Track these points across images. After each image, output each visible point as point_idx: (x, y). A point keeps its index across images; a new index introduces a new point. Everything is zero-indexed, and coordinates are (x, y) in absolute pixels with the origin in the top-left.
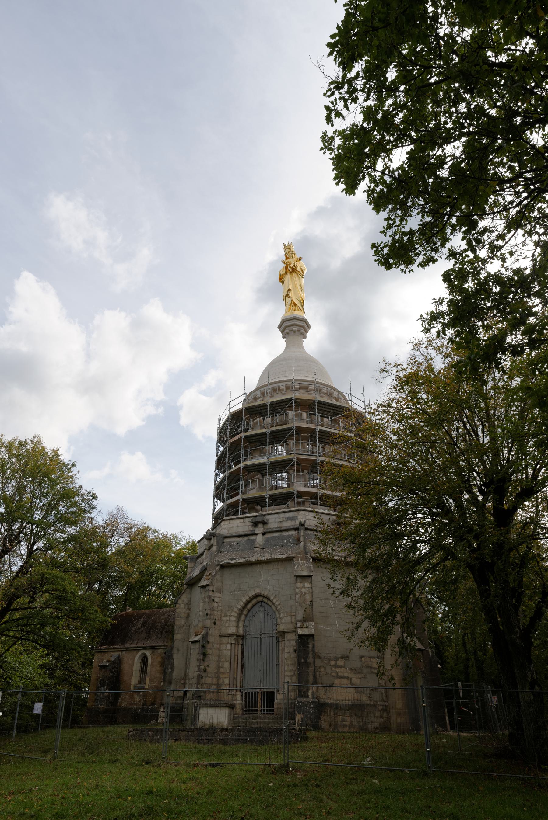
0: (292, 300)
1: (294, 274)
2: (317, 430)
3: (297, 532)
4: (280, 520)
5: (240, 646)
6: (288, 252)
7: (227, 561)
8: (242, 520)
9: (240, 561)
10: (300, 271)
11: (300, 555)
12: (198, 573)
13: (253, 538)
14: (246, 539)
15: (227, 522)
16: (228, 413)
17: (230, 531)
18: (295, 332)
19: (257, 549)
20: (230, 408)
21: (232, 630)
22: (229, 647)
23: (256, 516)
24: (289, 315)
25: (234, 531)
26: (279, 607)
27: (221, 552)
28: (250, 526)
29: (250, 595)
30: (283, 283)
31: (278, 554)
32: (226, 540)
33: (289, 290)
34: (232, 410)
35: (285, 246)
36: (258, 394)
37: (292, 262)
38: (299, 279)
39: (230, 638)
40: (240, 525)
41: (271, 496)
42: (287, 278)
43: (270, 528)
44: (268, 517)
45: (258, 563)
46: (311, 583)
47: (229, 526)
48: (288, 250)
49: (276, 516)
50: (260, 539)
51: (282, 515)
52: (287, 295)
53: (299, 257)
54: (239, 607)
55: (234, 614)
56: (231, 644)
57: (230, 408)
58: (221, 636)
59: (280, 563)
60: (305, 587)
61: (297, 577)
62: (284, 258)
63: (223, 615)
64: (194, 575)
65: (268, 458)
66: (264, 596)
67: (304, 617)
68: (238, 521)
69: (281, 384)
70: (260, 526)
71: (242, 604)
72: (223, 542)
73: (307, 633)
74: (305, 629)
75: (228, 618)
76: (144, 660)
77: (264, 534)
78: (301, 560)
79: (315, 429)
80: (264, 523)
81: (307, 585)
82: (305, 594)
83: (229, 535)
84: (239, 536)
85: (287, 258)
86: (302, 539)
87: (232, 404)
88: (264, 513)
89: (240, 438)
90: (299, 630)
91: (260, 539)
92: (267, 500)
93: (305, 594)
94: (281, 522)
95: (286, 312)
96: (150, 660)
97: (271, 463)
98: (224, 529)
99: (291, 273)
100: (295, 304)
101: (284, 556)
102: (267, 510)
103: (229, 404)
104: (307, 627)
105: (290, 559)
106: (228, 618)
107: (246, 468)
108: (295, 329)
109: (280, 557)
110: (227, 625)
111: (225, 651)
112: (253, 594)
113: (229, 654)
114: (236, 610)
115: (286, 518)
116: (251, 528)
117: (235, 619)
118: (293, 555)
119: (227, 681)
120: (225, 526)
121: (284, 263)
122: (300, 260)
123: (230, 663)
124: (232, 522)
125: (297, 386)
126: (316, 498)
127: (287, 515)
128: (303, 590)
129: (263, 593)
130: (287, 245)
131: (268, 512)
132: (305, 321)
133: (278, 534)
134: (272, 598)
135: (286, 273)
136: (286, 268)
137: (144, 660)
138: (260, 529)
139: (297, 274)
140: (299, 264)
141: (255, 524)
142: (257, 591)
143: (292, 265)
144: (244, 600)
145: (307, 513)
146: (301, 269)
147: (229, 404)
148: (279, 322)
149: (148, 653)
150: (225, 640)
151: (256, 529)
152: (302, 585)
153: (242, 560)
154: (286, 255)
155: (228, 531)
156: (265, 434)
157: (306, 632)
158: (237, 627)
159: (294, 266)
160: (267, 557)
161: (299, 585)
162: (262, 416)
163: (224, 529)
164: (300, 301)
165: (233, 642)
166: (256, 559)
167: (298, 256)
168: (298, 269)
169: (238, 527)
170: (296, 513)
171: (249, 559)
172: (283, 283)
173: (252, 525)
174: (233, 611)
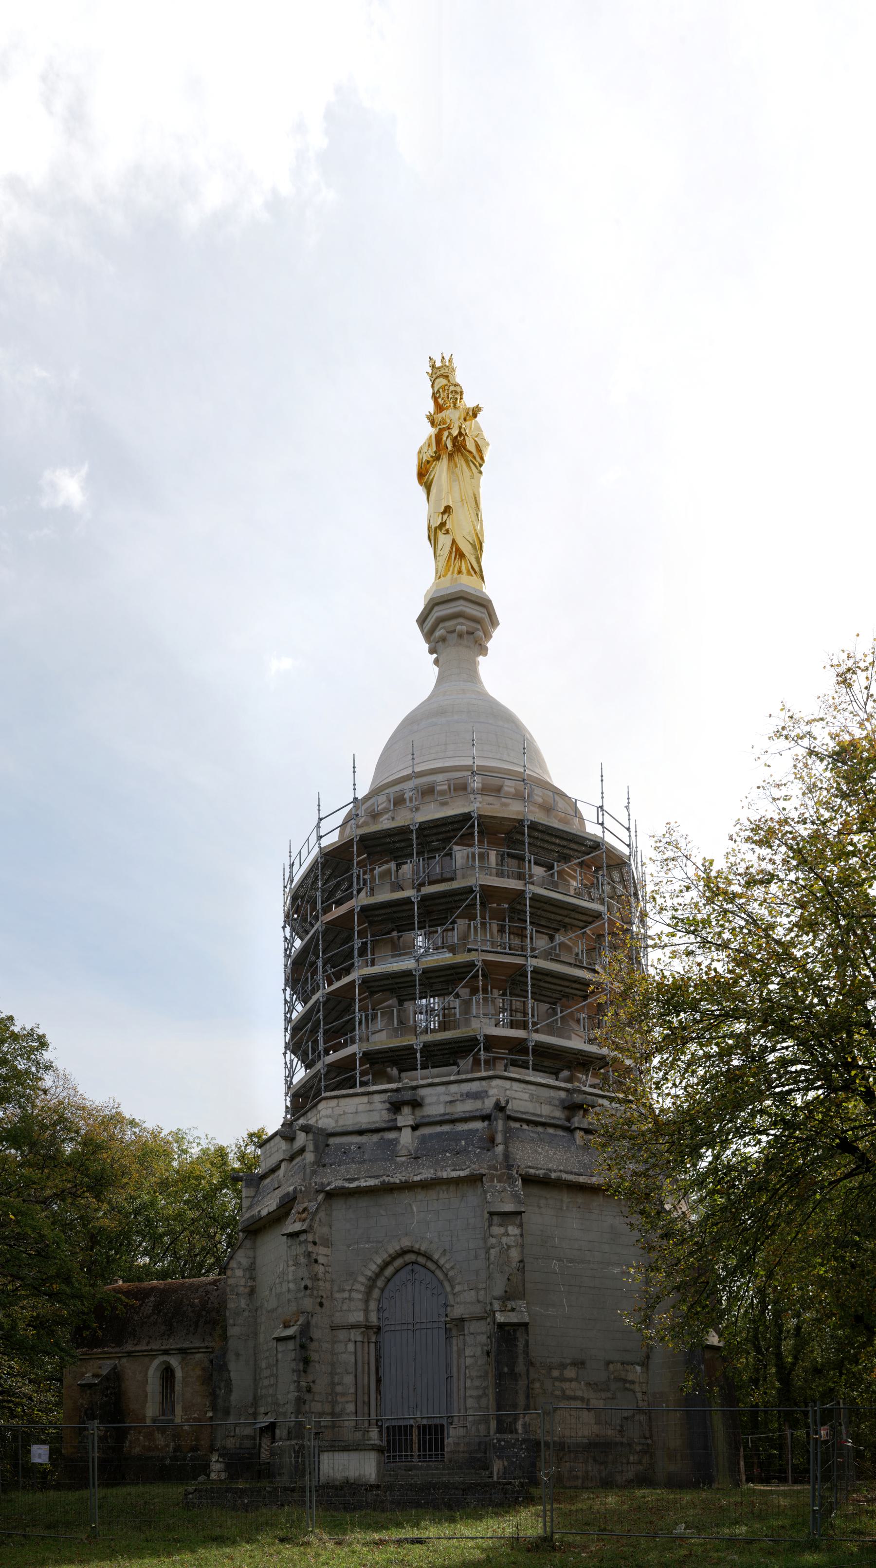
0: (454, 541)
1: (459, 460)
2: (528, 896)
3: (486, 1123)
4: (449, 1098)
5: (372, 1346)
6: (443, 388)
7: (339, 1183)
8: (365, 1099)
9: (368, 1184)
11: (496, 1170)
12: (273, 1207)
13: (392, 1135)
14: (376, 1137)
15: (333, 1103)
16: (316, 850)
17: (341, 1123)
19: (403, 1159)
20: (320, 837)
21: (357, 1317)
22: (351, 1347)
23: (397, 1090)
24: (449, 586)
25: (349, 1122)
26: (451, 1274)
27: (324, 1166)
28: (384, 1112)
29: (391, 1251)
30: (428, 487)
31: (449, 1169)
32: (332, 1141)
34: (325, 842)
35: (433, 366)
36: (381, 801)
38: (472, 477)
39: (353, 1331)
40: (361, 1108)
41: (426, 1046)
42: (441, 470)
43: (429, 1116)
44: (423, 1092)
45: (407, 1187)
46: (521, 1226)
47: (338, 1111)
49: (441, 1089)
50: (406, 1138)
51: (453, 1088)
52: (443, 524)
54: (369, 1273)
55: (357, 1286)
56: (356, 1342)
57: (320, 837)
58: (333, 1328)
59: (452, 1188)
60: (508, 1235)
61: (491, 1214)
62: (430, 407)
63: (336, 1288)
64: (264, 1213)
65: (417, 961)
66: (418, 1253)
67: (506, 1292)
68: (357, 1100)
69: (440, 778)
70: (406, 1110)
71: (374, 1267)
72: (328, 1145)
73: (515, 1320)
74: (510, 1313)
75: (346, 1295)
76: (168, 1374)
77: (414, 1128)
78: (499, 1181)
79: (524, 891)
80: (416, 1104)
81: (513, 1230)
82: (509, 1247)
83: (338, 1130)
84: (360, 1133)
85: (439, 408)
86: (499, 1138)
87: (325, 827)
88: (414, 1083)
89: (351, 912)
90: (498, 1315)
91: (406, 1138)
92: (418, 1055)
93: (509, 1247)
94: (451, 1102)
95: (439, 577)
96: (179, 1374)
97: (426, 971)
98: (327, 1117)
99: (451, 456)
100: (461, 555)
101: (462, 1174)
102: (419, 1077)
103: (318, 826)
104: (513, 1310)
105: (475, 1180)
106: (346, 1295)
107: (368, 983)
109: (454, 1174)
110: (345, 1307)
111: (344, 1356)
112: (398, 1248)
113: (353, 1360)
114: (362, 1279)
115: (462, 1095)
116: (385, 1115)
117: (360, 1296)
118: (483, 1171)
119: (351, 1408)
120: (329, 1112)
121: (433, 424)
123: (356, 1376)
124: (343, 1102)
125: (476, 783)
126: (524, 1051)
127: (466, 1087)
128: (505, 1240)
129: (417, 1246)
130: (438, 364)
131: (421, 1082)
132: (485, 604)
133: (446, 1128)
134: (436, 1257)
135: (437, 458)
136: (438, 438)
137: (168, 1374)
138: (406, 1118)
139: (467, 461)
141: (396, 1107)
142: (406, 1243)
143: (455, 432)
144: (379, 1261)
145: (507, 1084)
146: (477, 446)
147: (318, 826)
149: (174, 1361)
150: (342, 1335)
151: (399, 1118)
152: (502, 1230)
153: (372, 1182)
154: (435, 397)
155: (337, 1121)
156: (408, 901)
157: (513, 1318)
158: (366, 1311)
159: (460, 434)
160: (426, 1174)
161: (497, 1230)
162: (395, 858)
163: (327, 1117)
164: (474, 546)
165: (359, 1338)
166: (403, 1179)
167: (469, 401)
168: (470, 446)
169: (356, 1113)
170: (484, 1083)
171: (386, 1179)
173: (388, 1109)
174: (355, 1280)
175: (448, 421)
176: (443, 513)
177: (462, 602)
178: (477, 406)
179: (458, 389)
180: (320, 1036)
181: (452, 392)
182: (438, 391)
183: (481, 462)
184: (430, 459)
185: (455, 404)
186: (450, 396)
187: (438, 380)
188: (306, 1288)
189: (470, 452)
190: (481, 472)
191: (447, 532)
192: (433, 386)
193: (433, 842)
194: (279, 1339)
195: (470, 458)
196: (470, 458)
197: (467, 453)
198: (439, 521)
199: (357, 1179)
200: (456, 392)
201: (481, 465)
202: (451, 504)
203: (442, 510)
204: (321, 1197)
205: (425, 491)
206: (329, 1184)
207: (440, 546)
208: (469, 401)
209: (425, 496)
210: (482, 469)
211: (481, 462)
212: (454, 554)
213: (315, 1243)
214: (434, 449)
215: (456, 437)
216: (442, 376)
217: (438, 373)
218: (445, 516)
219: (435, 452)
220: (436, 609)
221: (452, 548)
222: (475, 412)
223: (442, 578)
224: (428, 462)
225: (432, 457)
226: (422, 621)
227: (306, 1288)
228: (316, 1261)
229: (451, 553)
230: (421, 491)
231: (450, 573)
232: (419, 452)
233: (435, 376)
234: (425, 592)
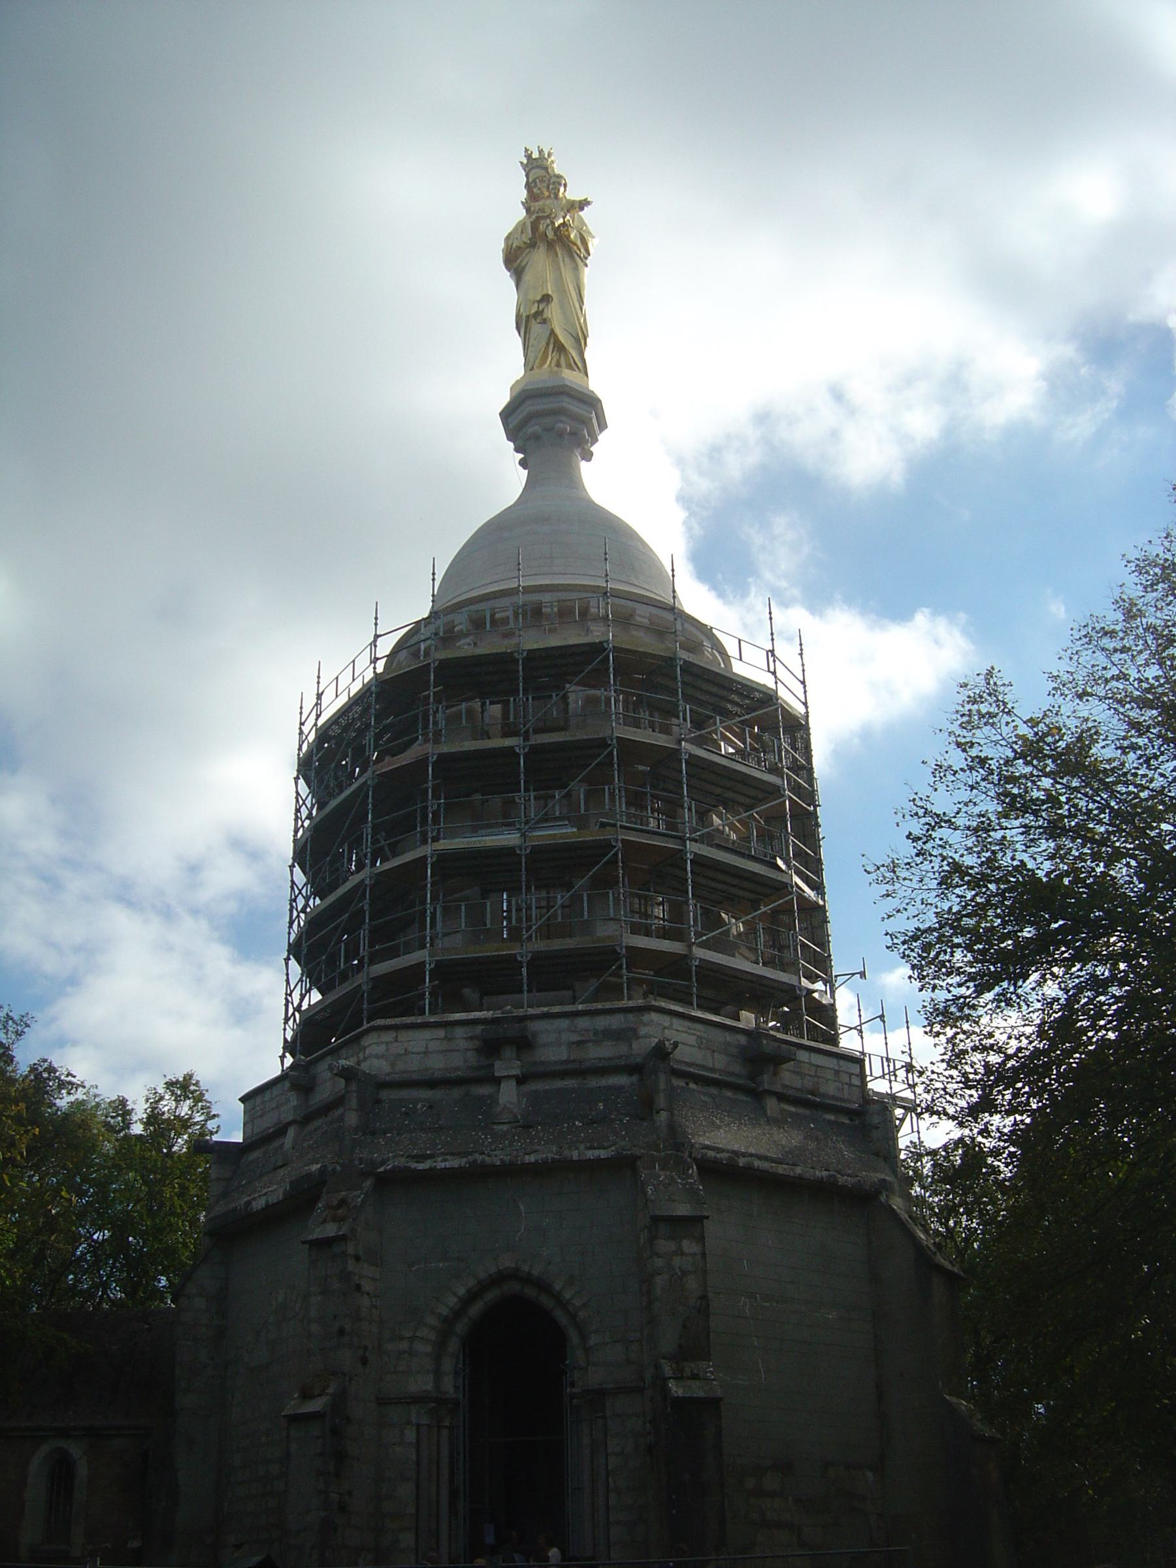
0: (552, 332)
2: (685, 757)
3: (635, 1078)
4: (575, 1038)
8: (441, 1033)
9: (448, 1164)
11: (658, 1150)
13: (484, 1090)
14: (457, 1093)
15: (388, 1037)
17: (400, 1066)
19: (505, 1127)
23: (494, 1021)
25: (414, 1066)
27: (373, 1133)
28: (471, 1055)
31: (582, 1147)
32: (385, 1094)
33: (546, 299)
36: (461, 622)
40: (433, 1046)
41: (537, 960)
43: (543, 1063)
44: (534, 1026)
45: (512, 1172)
46: (701, 1239)
47: (397, 1048)
48: (542, 173)
49: (564, 1023)
50: (508, 1094)
51: (583, 1023)
52: (538, 314)
60: (683, 1254)
62: (524, 194)
67: (680, 1346)
68: (427, 1034)
69: (546, 597)
70: (509, 1052)
72: (378, 1101)
74: (689, 1383)
77: (521, 1080)
78: (663, 1168)
80: (524, 1044)
81: (689, 1246)
82: (685, 1273)
83: (397, 1077)
84: (432, 1084)
86: (661, 1100)
88: (520, 1012)
91: (508, 1094)
92: (524, 971)
93: (685, 1273)
94: (579, 1043)
97: (535, 850)
98: (377, 1057)
100: (560, 348)
101: (603, 1154)
102: (526, 1005)
104: (695, 1377)
105: (625, 1165)
107: (445, 861)
109: (591, 1154)
115: (596, 1033)
116: (472, 1058)
118: (637, 1151)
120: (381, 1049)
124: (404, 1036)
127: (602, 1022)
128: (677, 1261)
130: (535, 155)
131: (531, 1011)
133: (569, 1083)
135: (532, 245)
138: (507, 1066)
141: (490, 1047)
145: (665, 1020)
148: (504, 399)
151: (498, 1064)
152: (672, 1246)
153: (454, 1163)
155: (393, 1065)
160: (546, 1152)
163: (377, 1057)
166: (507, 1159)
167: (572, 193)
169: (426, 1053)
170: (630, 1017)
171: (479, 1158)
173: (477, 1050)
175: (548, 212)
176: (540, 302)
178: (586, 200)
180: (364, 933)
181: (554, 183)
182: (534, 181)
183: (586, 255)
186: (551, 187)
187: (533, 172)
188: (341, 1332)
190: (586, 265)
192: (527, 176)
193: (541, 677)
194: (296, 1419)
197: (571, 244)
199: (431, 1157)
201: (586, 258)
202: (550, 293)
203: (538, 298)
204: (368, 1183)
205: (514, 277)
206: (383, 1163)
207: (533, 336)
208: (572, 193)
210: (587, 262)
211: (586, 255)
212: (551, 347)
213: (357, 1258)
214: (530, 235)
216: (537, 167)
217: (535, 164)
219: (530, 239)
220: (529, 402)
221: (549, 339)
222: (583, 204)
223: (536, 371)
225: (525, 243)
227: (341, 1332)
228: (358, 1288)
229: (548, 344)
231: (546, 366)
232: (507, 238)
233: (530, 166)
234: (513, 382)
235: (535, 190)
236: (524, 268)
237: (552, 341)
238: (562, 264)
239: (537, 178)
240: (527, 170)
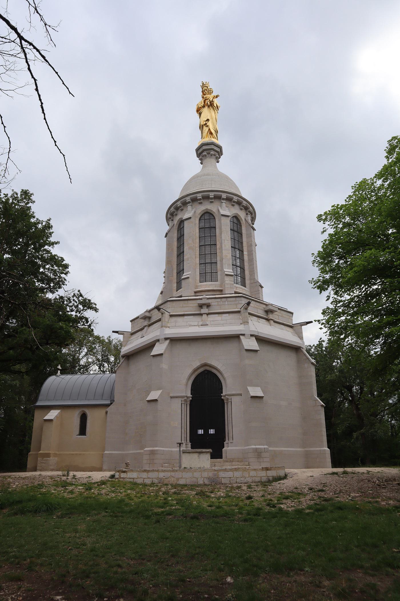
0: (209, 129)
10: (216, 106)
18: (211, 155)
30: (200, 114)
33: (208, 120)
37: (210, 97)
42: (205, 111)
48: (206, 88)
52: (206, 124)
53: (216, 95)
108: (212, 152)
122: (217, 97)
130: (205, 83)
132: (220, 147)
135: (204, 107)
140: (216, 102)
148: (197, 146)
159: (212, 101)
164: (215, 131)
172: (200, 114)
176: (206, 121)
177: (213, 146)
179: (211, 90)
181: (210, 90)
184: (201, 107)
185: (210, 94)
186: (209, 91)
189: (215, 106)
191: (207, 126)
192: (202, 89)
195: (215, 108)
196: (215, 108)
198: (205, 123)
200: (211, 91)
205: (199, 115)
209: (199, 117)
212: (209, 133)
215: (211, 102)
216: (206, 87)
217: (205, 86)
218: (207, 122)
219: (203, 105)
220: (203, 146)
221: (208, 131)
224: (200, 107)
225: (202, 106)
226: (197, 150)
229: (208, 132)
230: (197, 115)
232: (197, 105)
235: (204, 93)
236: (202, 112)
237: (209, 131)
238: (212, 112)
239: (205, 89)
240: (202, 87)
